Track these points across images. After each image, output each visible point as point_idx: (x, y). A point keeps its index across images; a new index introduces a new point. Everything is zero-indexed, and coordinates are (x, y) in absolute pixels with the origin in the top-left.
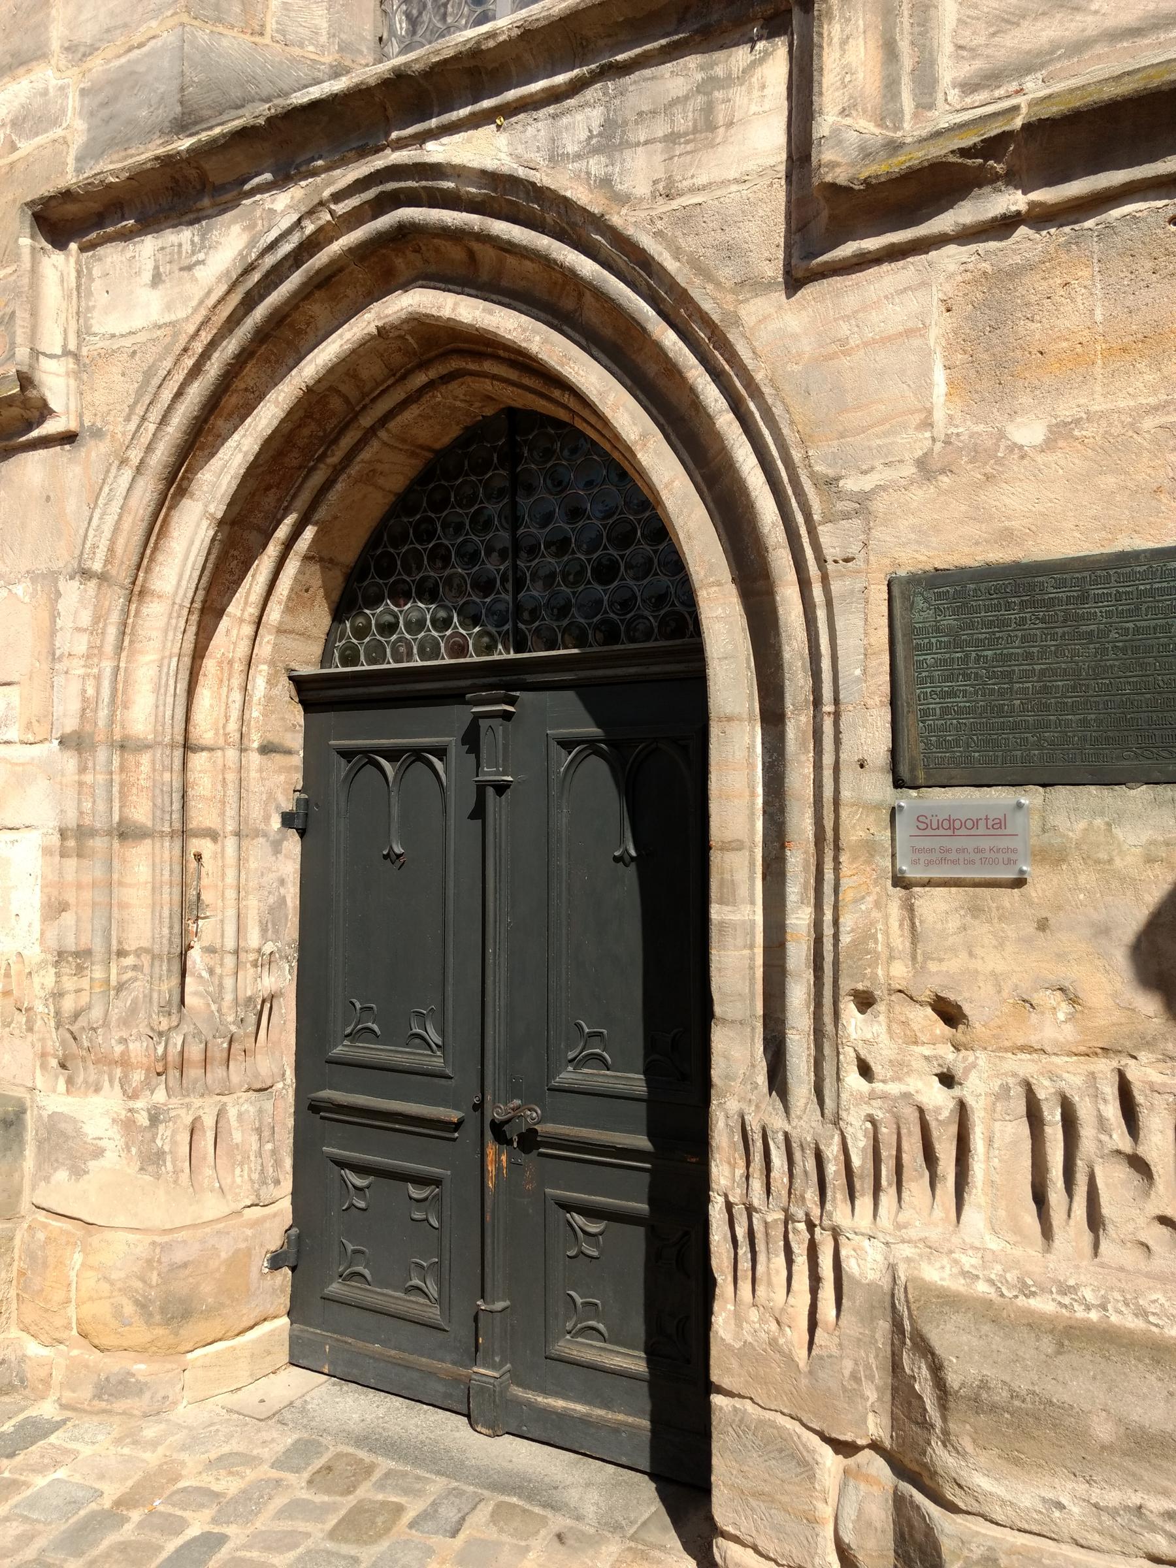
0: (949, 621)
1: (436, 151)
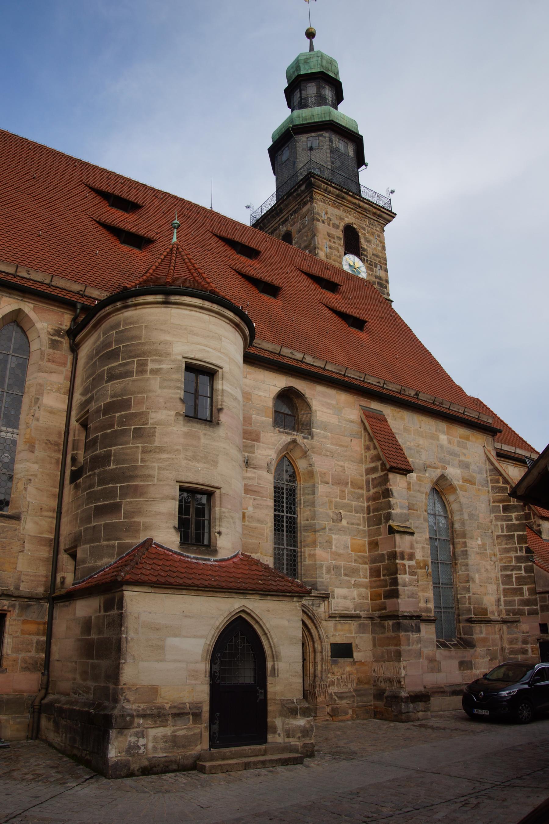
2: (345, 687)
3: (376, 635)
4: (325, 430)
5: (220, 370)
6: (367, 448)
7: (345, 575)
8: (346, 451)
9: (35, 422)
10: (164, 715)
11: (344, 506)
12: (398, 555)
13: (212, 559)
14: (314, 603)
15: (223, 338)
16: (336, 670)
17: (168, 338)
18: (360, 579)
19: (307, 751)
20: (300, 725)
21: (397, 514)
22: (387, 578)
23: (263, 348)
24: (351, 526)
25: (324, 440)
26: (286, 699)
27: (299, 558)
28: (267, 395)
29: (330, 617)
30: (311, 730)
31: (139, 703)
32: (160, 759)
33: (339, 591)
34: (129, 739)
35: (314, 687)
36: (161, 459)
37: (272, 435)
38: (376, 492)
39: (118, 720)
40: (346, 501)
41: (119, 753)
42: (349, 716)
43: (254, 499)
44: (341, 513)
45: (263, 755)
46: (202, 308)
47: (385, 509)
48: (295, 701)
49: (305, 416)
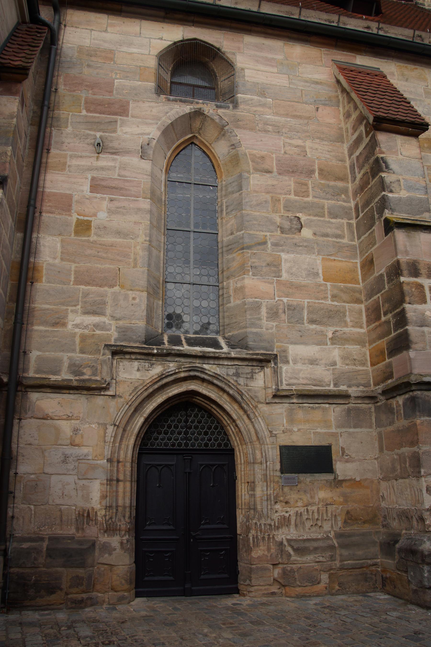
0: (287, 452)
1: (205, 366)
2: (314, 529)
3: (382, 429)
4: (263, 93)
6: (348, 116)
7: (312, 321)
8: (307, 124)
11: (305, 208)
12: (404, 266)
14: (240, 371)
16: (293, 496)
18: (346, 329)
21: (400, 199)
22: (390, 316)
24: (321, 239)
25: (259, 109)
28: (147, 52)
29: (275, 396)
33: (295, 350)
35: (248, 529)
37: (153, 104)
38: (364, 175)
40: (310, 199)
42: (322, 585)
44: (299, 218)
47: (376, 196)
49: (226, 82)
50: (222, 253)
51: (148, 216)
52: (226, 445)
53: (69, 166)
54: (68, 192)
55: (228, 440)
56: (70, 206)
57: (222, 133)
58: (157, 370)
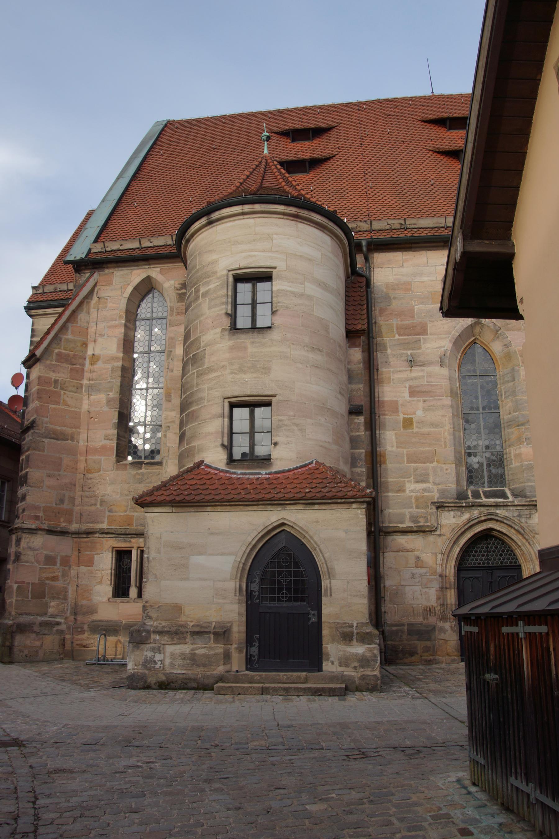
1: (497, 511)
5: (274, 271)
9: (170, 374)
10: (182, 633)
13: (264, 472)
14: (522, 513)
15: (275, 236)
17: (213, 257)
19: (368, 684)
20: (357, 653)
23: (421, 226)
26: (342, 622)
27: (505, 461)
28: (434, 279)
30: (373, 660)
31: (162, 620)
32: (178, 675)
34: (146, 653)
36: (209, 380)
39: (134, 635)
41: (136, 665)
43: (424, 401)
45: (303, 683)
46: (243, 214)
48: (355, 625)
50: (504, 427)
51: (450, 410)
52: (515, 562)
53: (393, 379)
54: (395, 399)
55: (517, 559)
56: (397, 408)
57: (497, 336)
58: (466, 516)
